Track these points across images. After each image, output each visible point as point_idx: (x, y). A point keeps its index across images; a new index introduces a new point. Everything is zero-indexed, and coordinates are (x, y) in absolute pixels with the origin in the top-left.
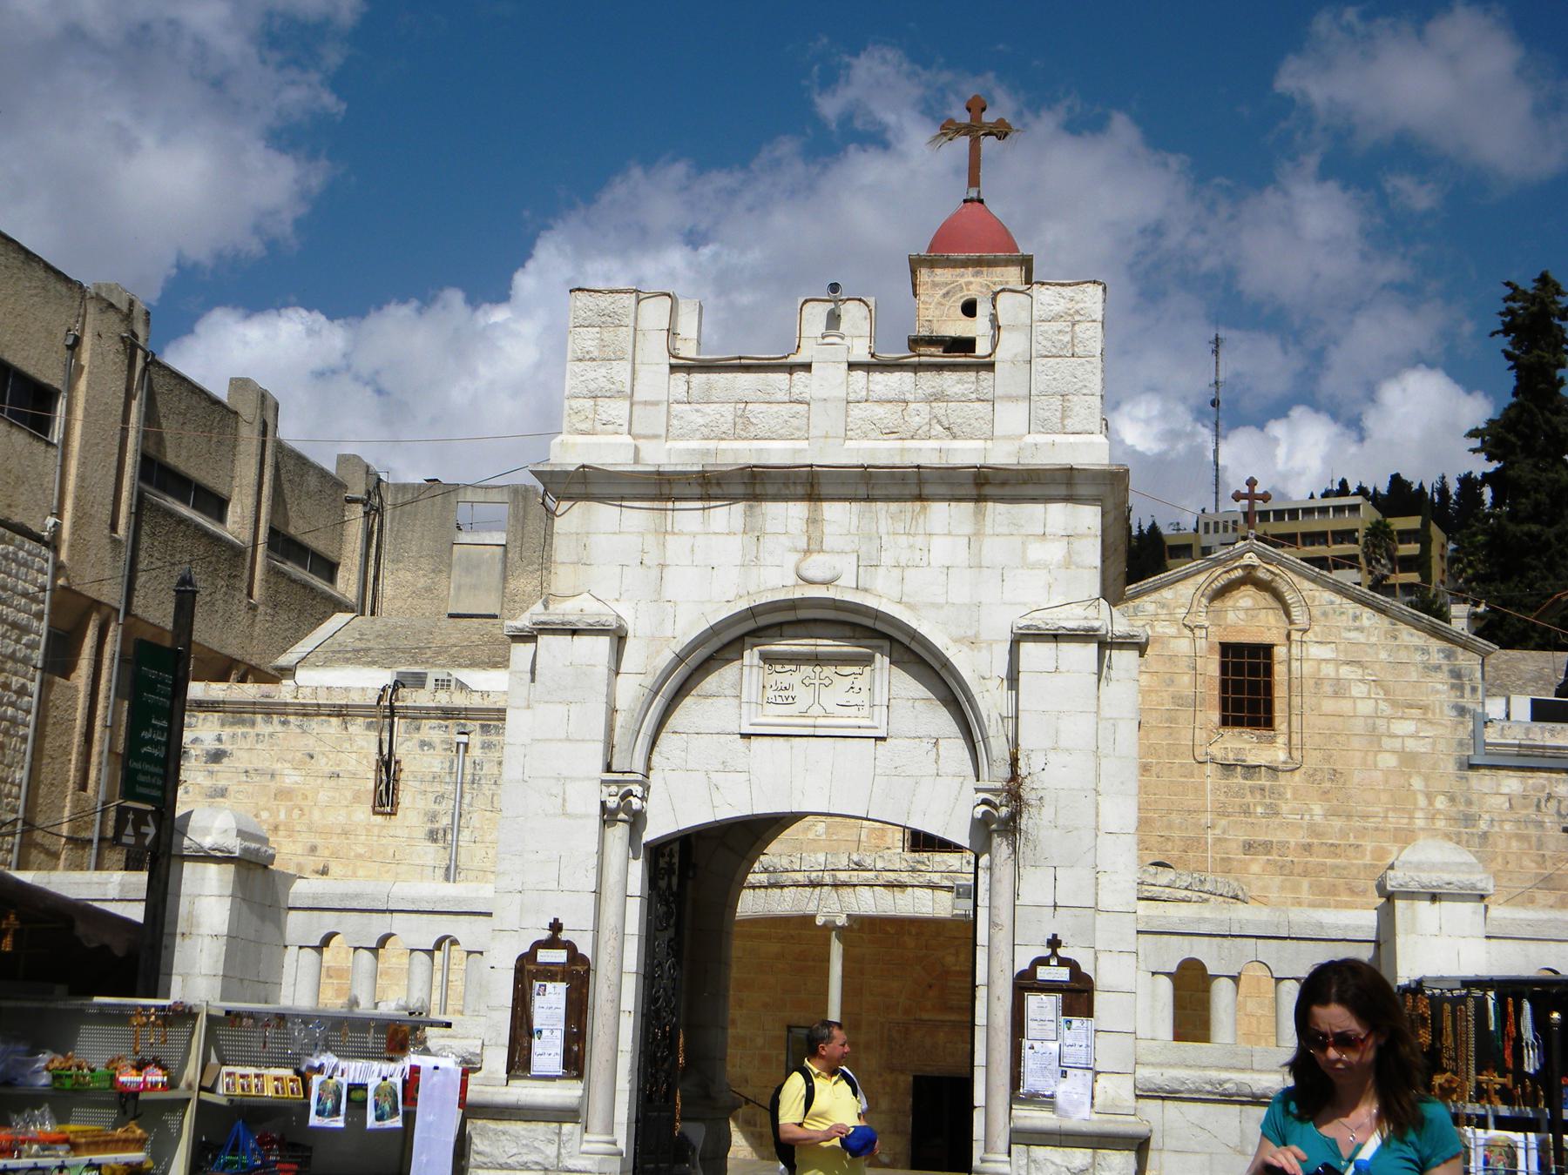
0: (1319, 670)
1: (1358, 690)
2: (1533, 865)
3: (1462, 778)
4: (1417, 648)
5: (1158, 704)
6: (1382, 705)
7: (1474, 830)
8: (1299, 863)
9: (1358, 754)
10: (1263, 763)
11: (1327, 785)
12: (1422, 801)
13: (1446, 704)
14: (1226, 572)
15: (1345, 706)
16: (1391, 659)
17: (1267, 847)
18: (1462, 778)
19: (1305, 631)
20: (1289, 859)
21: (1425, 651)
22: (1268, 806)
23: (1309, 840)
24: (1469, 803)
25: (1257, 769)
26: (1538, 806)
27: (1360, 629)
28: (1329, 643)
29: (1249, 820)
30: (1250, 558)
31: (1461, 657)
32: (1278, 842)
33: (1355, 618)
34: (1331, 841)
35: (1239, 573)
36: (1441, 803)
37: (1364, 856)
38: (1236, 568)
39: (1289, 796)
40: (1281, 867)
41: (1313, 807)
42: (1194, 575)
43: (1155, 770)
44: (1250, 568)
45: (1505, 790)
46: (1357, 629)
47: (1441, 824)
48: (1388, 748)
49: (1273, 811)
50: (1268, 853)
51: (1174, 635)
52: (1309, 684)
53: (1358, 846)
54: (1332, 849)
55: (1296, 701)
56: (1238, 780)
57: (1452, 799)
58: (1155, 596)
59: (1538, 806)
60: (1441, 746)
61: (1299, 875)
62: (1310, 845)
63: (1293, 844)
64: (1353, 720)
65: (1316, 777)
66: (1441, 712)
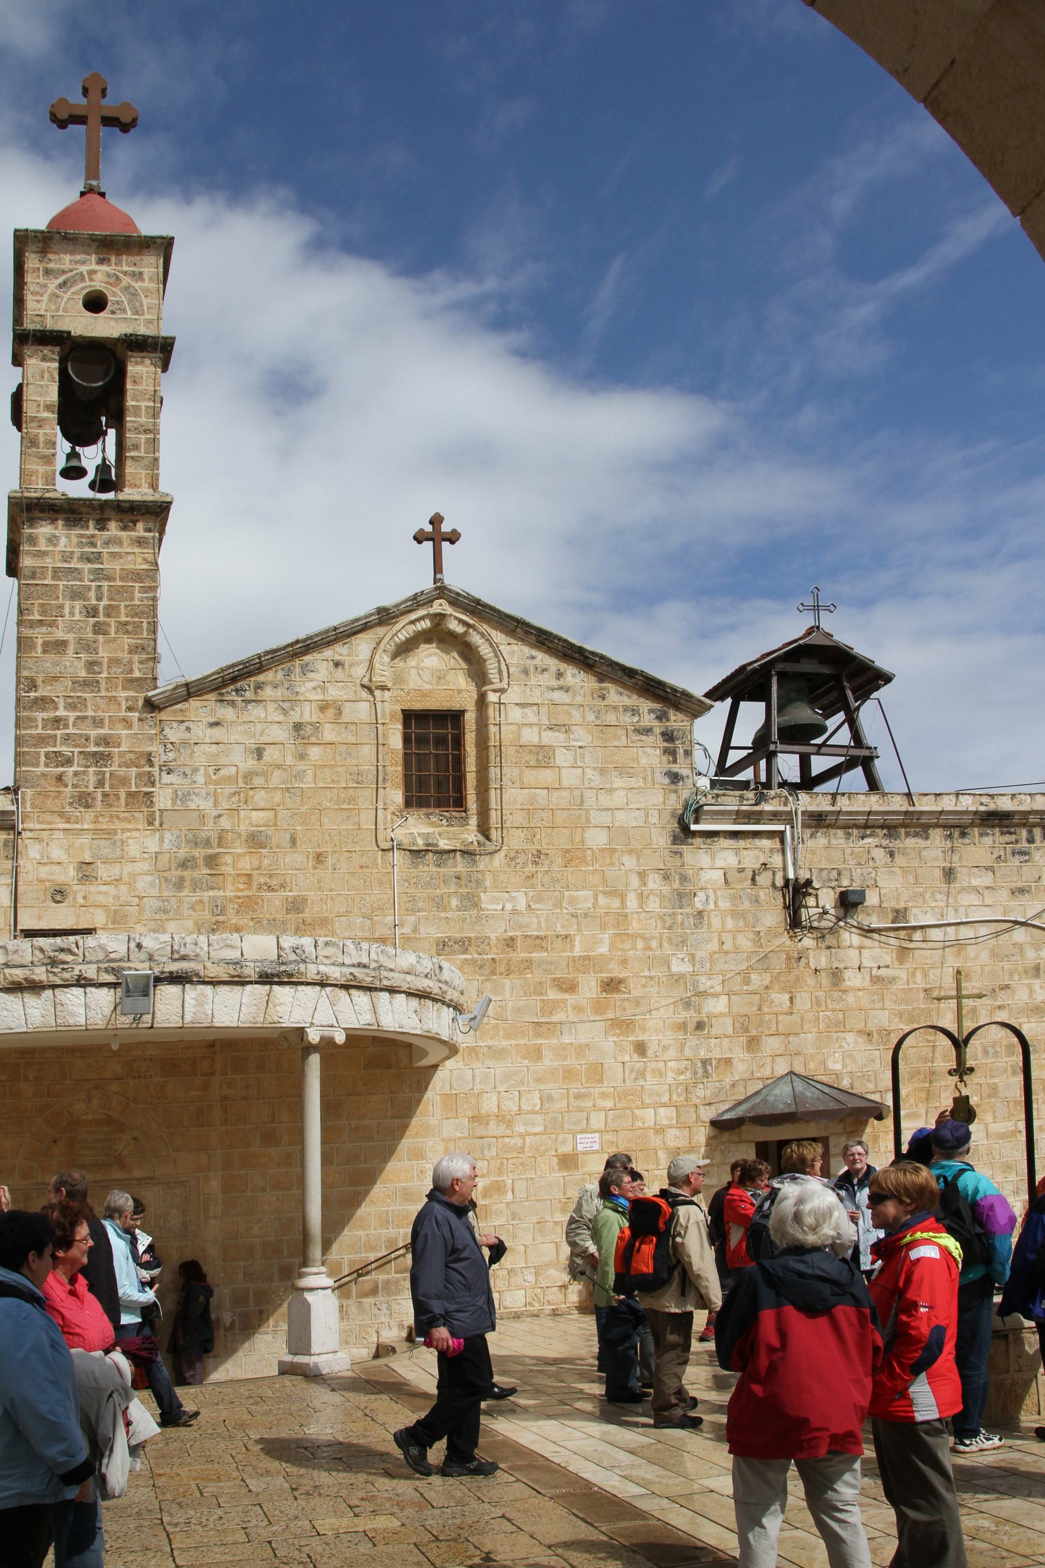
0: (519, 736)
1: (563, 758)
2: (750, 944)
3: (676, 853)
4: (626, 709)
5: (333, 781)
6: (589, 772)
7: (688, 910)
8: (501, 960)
9: (565, 831)
10: (459, 847)
11: (531, 868)
12: (635, 882)
13: (657, 771)
14: (413, 622)
15: (547, 776)
16: (599, 722)
17: (464, 944)
18: (676, 853)
19: (502, 691)
20: (489, 956)
21: (634, 711)
22: (463, 897)
23: (511, 934)
24: (684, 879)
25: (451, 855)
26: (753, 879)
27: (566, 689)
28: (532, 705)
29: (443, 915)
30: (441, 605)
31: (673, 718)
32: (477, 938)
33: (560, 675)
34: (536, 933)
35: (426, 624)
36: (654, 882)
37: (572, 949)
38: (422, 618)
39: (488, 884)
40: (481, 967)
41: (514, 894)
42: (372, 627)
43: (330, 861)
44: (441, 617)
45: (719, 863)
46: (561, 688)
47: (654, 904)
48: (597, 823)
49: (471, 902)
50: (465, 951)
51: (351, 698)
52: (509, 752)
53: (566, 937)
54: (538, 941)
55: (493, 772)
56: (428, 867)
57: (666, 877)
58: (328, 653)
59: (753, 879)
60: (654, 819)
61: (501, 974)
62: (512, 939)
63: (494, 938)
64: (556, 793)
65: (518, 861)
66: (653, 779)
